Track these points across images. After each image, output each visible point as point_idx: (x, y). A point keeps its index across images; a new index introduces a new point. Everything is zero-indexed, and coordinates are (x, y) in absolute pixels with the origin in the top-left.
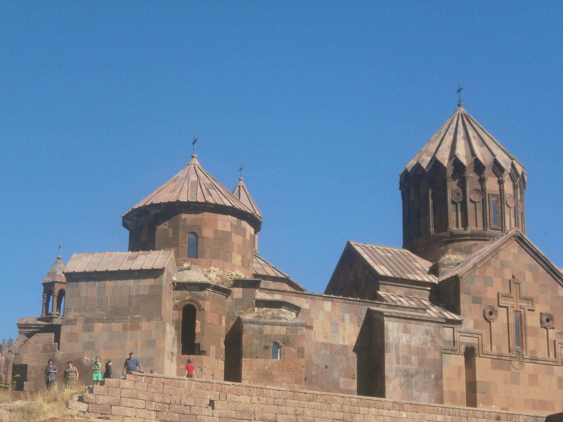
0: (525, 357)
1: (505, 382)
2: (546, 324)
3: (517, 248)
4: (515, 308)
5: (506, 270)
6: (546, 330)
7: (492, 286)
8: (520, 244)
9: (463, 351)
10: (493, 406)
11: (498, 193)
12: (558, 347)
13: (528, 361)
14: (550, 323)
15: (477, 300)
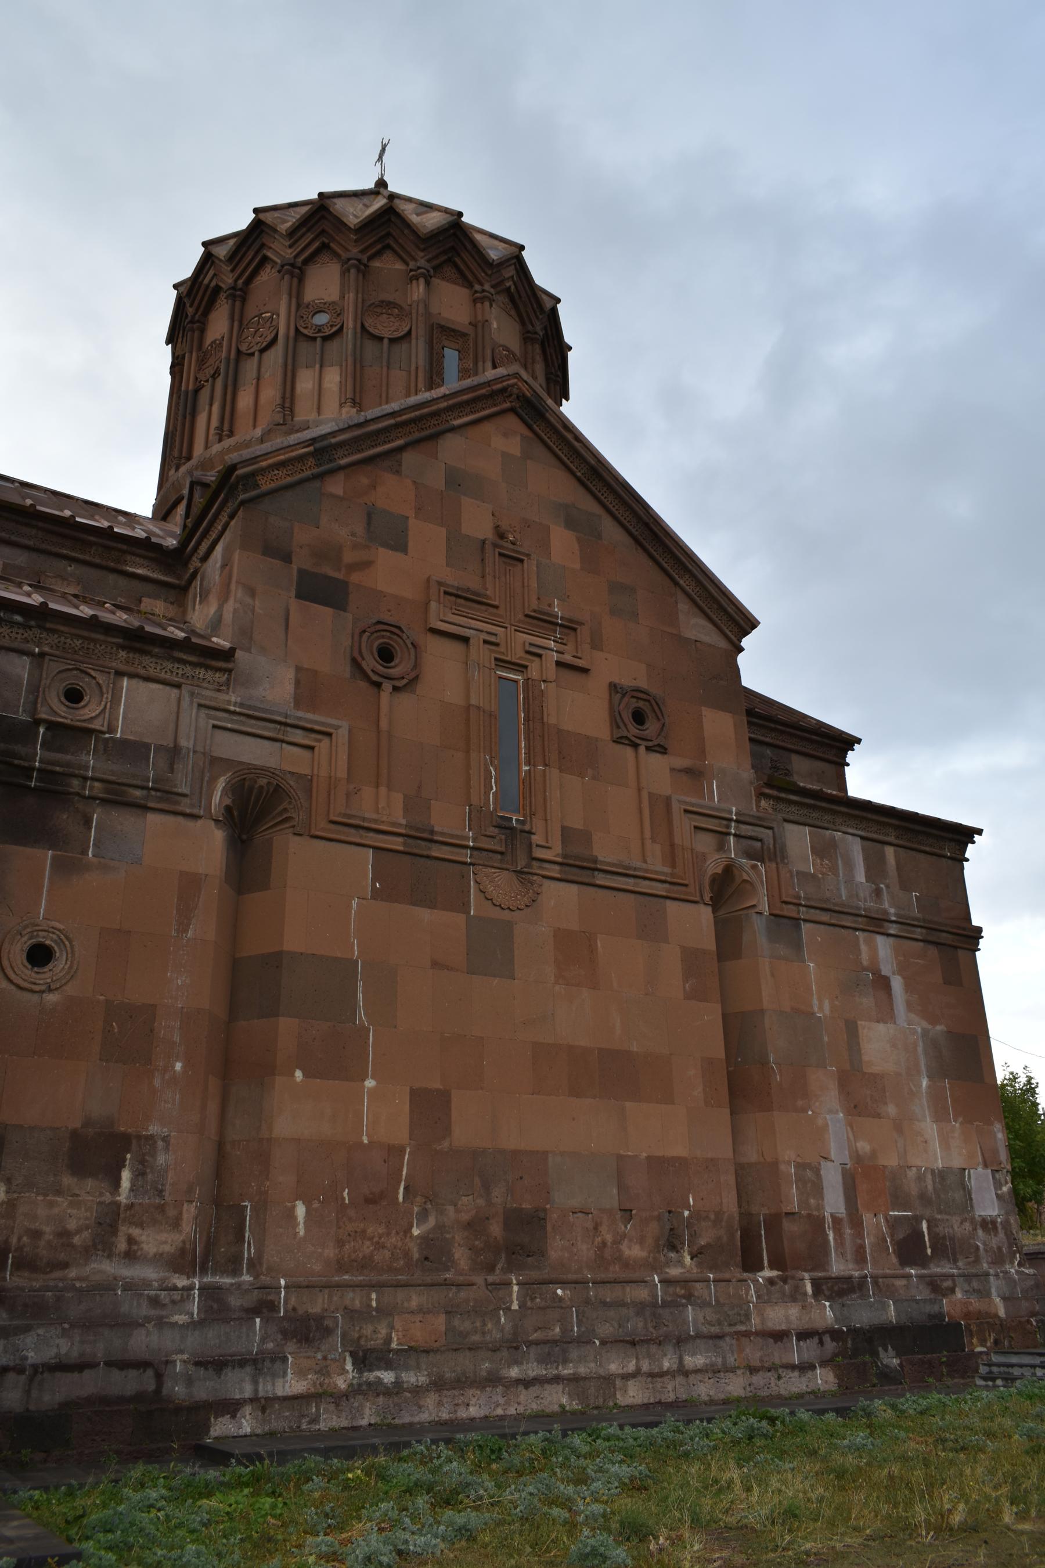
0: (539, 853)
1: (435, 964)
2: (633, 730)
3: (518, 438)
4: (502, 649)
5: (466, 501)
6: (629, 751)
7: (400, 545)
8: (530, 427)
9: (218, 797)
10: (370, 1083)
11: (470, 330)
12: (683, 826)
13: (555, 871)
14: (651, 727)
15: (321, 590)
